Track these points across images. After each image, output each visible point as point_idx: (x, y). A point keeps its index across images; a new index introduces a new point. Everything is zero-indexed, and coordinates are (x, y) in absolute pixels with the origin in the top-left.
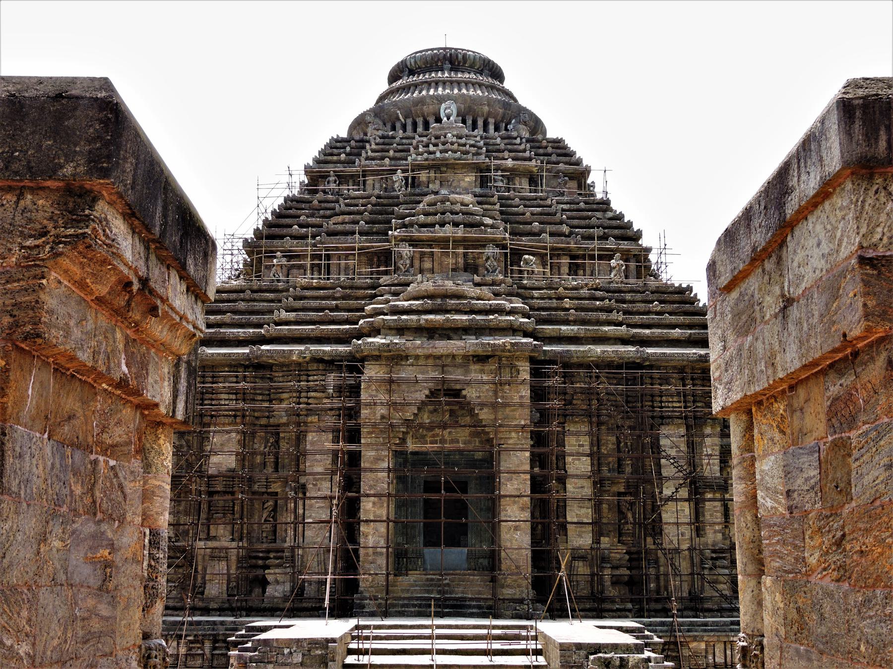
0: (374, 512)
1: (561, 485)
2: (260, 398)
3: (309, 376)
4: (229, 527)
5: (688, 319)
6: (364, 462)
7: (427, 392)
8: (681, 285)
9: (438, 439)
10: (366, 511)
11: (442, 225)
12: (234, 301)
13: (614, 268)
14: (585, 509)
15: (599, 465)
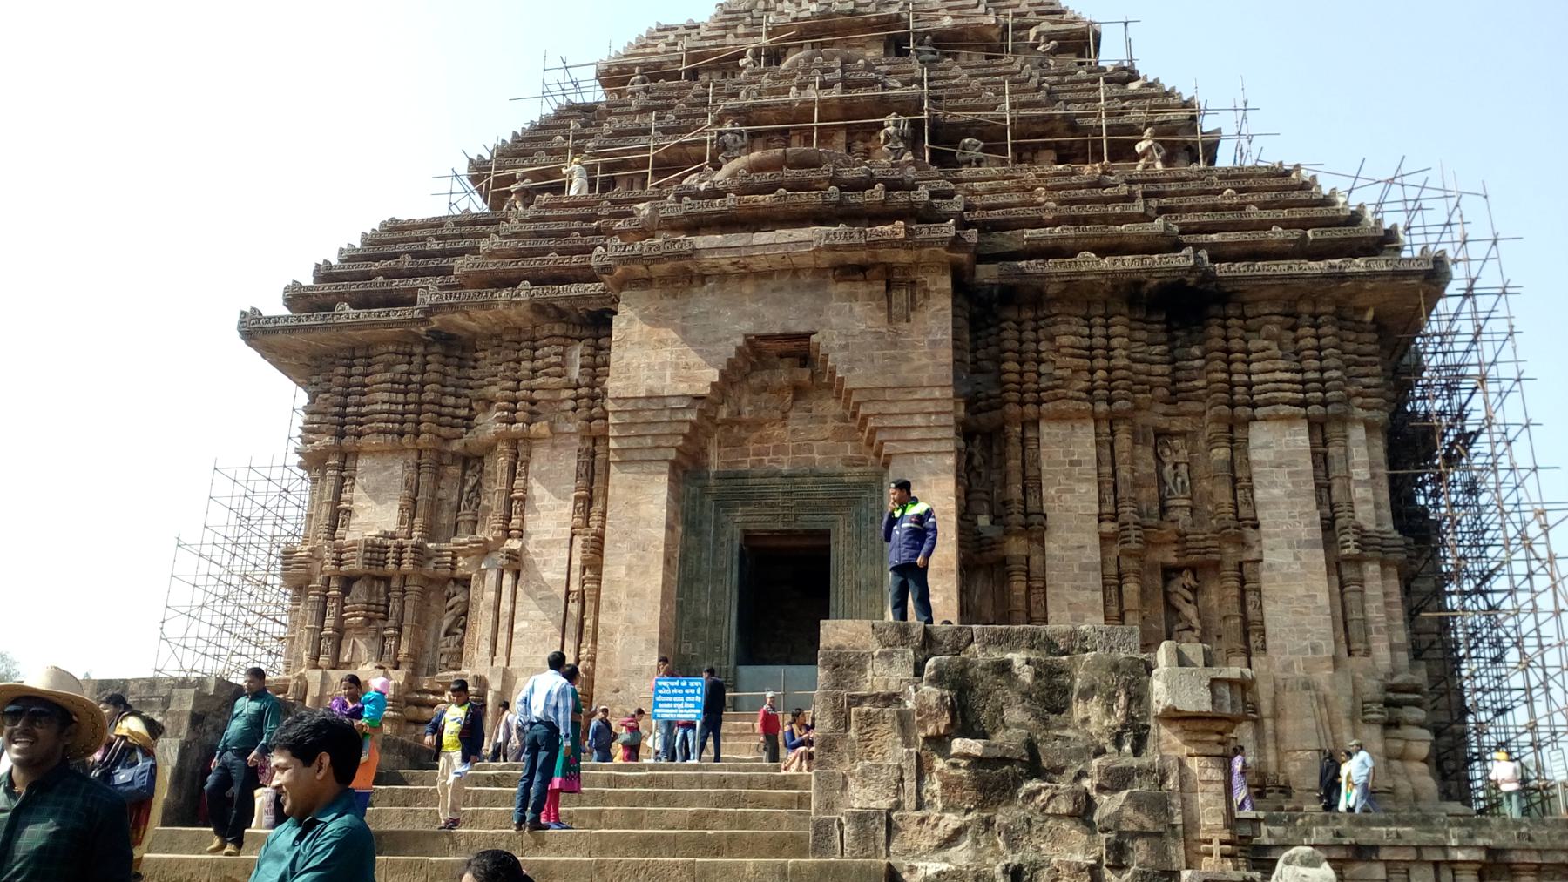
0: (630, 584)
1: (1035, 546)
2: (451, 400)
3: (535, 349)
4: (375, 646)
5: (1299, 214)
6: (614, 486)
7: (740, 341)
8: (1281, 163)
9: (771, 445)
10: (611, 581)
11: (802, 86)
12: (424, 239)
13: (1144, 154)
14: (1088, 593)
15: (1116, 502)
